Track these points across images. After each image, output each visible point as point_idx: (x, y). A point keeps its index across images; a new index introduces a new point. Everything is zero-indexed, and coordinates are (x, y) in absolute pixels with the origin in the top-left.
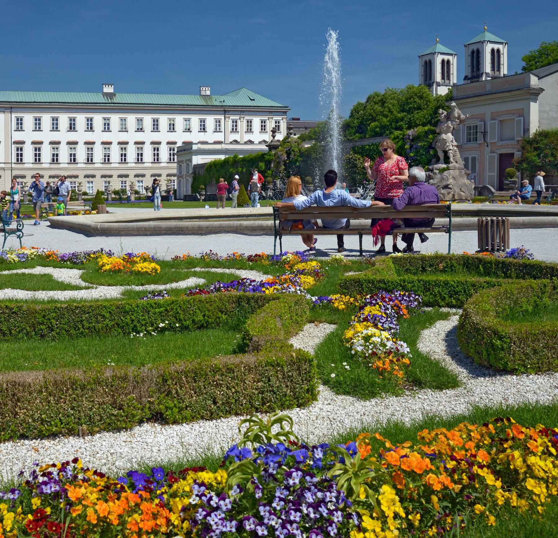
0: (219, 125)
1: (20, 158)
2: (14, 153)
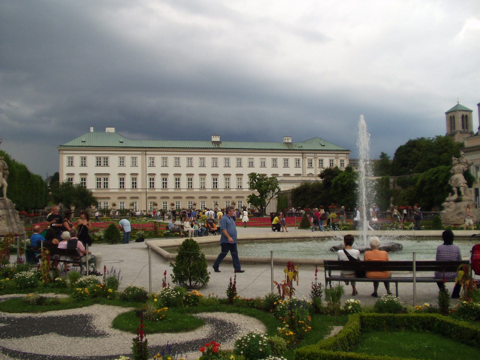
0: (299, 163)
1: (152, 185)
2: (148, 181)
